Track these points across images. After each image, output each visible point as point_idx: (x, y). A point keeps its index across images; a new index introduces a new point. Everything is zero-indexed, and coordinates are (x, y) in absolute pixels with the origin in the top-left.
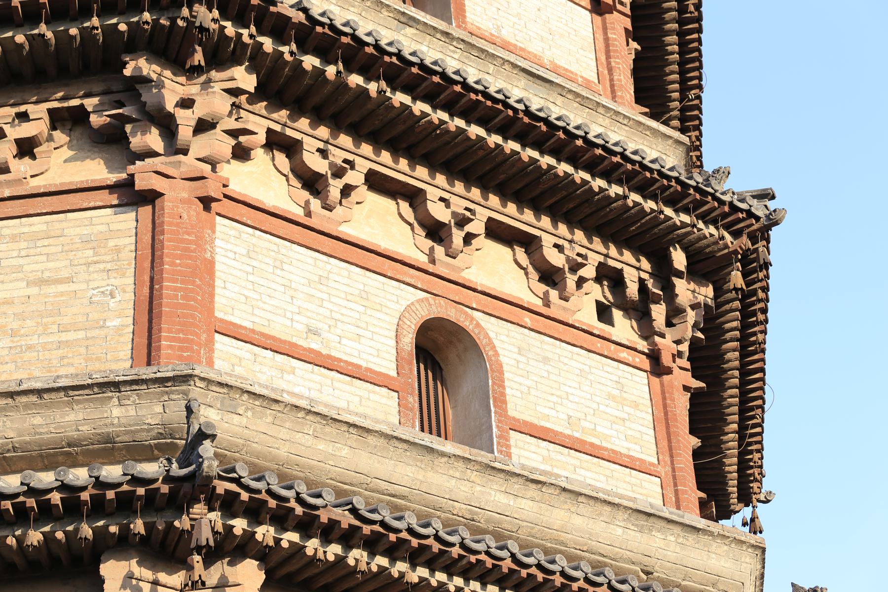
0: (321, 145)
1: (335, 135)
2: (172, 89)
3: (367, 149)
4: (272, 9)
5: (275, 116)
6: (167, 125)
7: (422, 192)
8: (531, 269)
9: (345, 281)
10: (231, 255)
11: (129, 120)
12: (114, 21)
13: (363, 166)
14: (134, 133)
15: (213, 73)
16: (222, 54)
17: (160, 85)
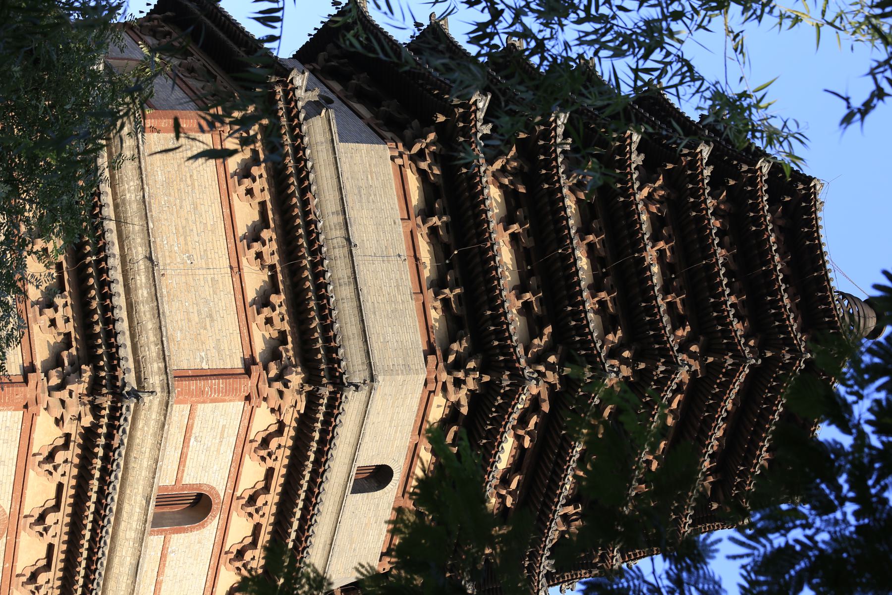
0: (69, 460)
1: (76, 466)
2: (80, 388)
3: (73, 482)
4: (115, 432)
5: (78, 437)
6: (60, 387)
7: (59, 510)
8: (36, 567)
9: (5, 474)
10: (5, 419)
11: (63, 369)
12: (105, 359)
13: (64, 480)
14: (57, 372)
15: (89, 406)
16: (96, 410)
17: (80, 382)
